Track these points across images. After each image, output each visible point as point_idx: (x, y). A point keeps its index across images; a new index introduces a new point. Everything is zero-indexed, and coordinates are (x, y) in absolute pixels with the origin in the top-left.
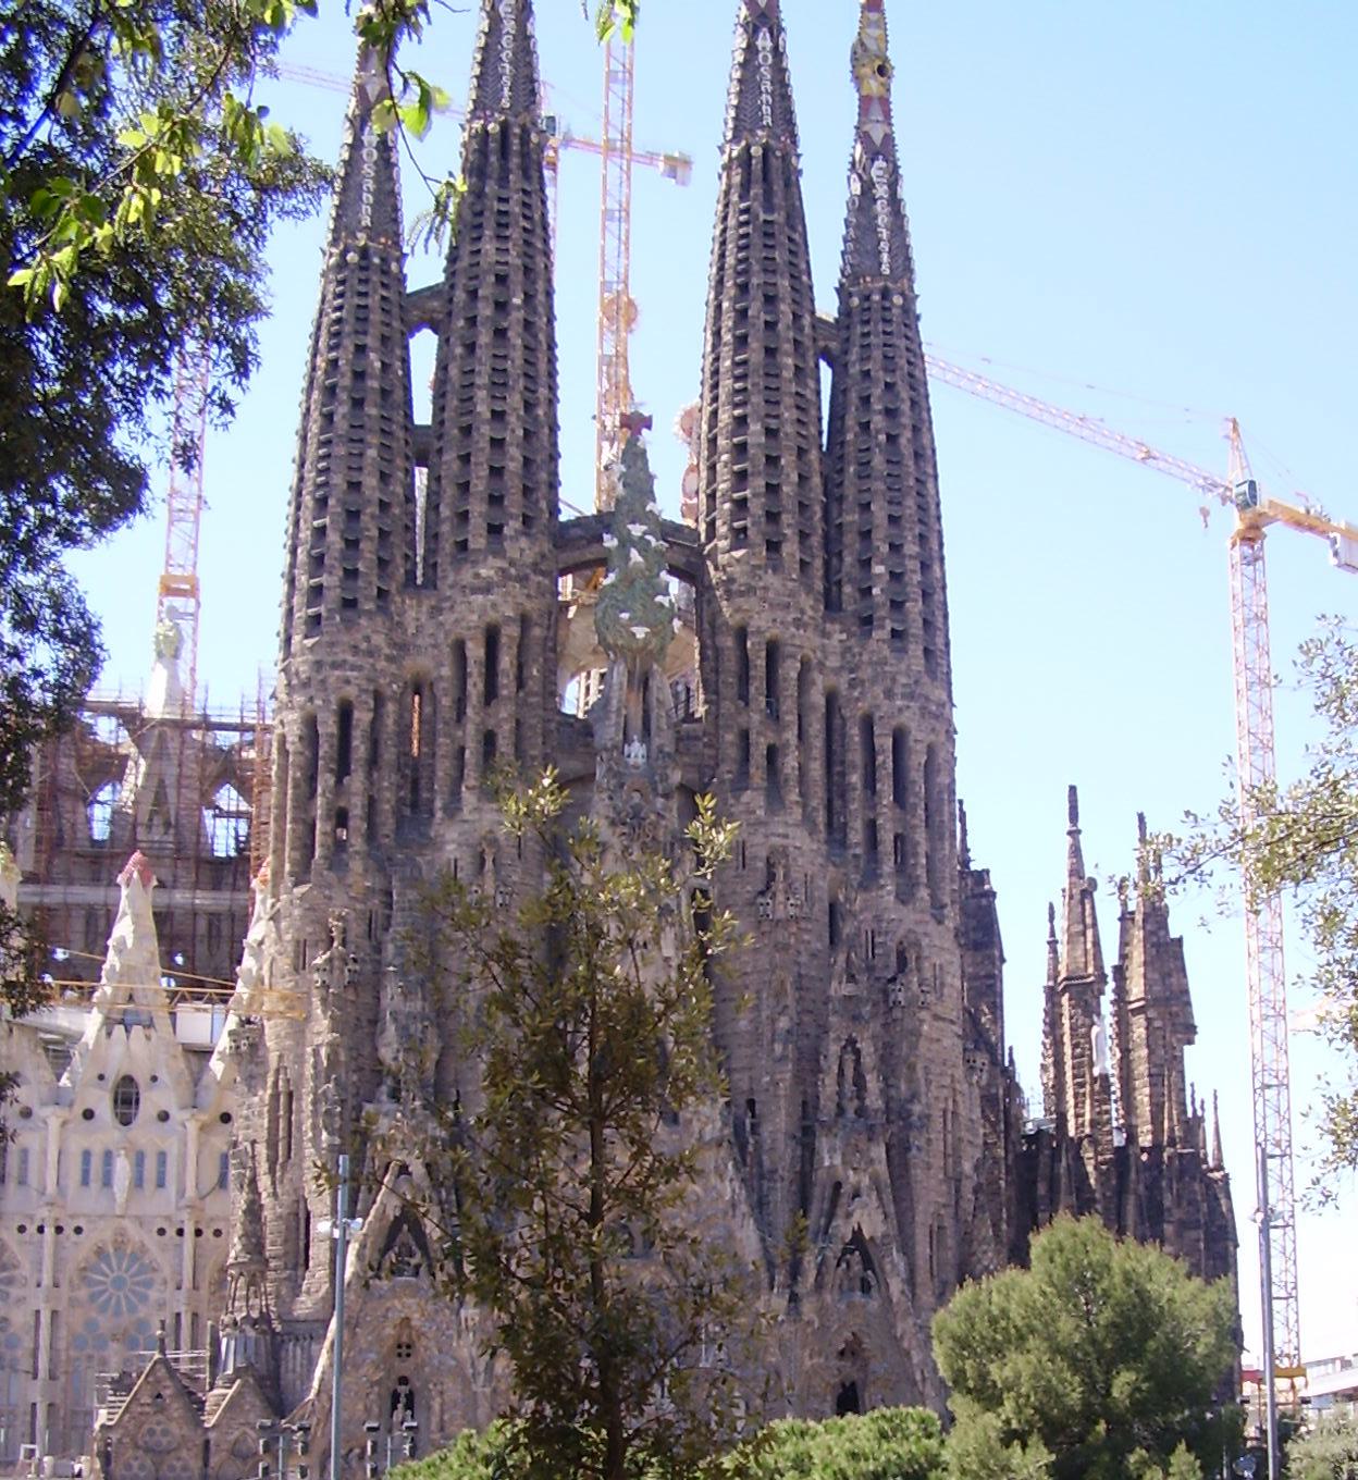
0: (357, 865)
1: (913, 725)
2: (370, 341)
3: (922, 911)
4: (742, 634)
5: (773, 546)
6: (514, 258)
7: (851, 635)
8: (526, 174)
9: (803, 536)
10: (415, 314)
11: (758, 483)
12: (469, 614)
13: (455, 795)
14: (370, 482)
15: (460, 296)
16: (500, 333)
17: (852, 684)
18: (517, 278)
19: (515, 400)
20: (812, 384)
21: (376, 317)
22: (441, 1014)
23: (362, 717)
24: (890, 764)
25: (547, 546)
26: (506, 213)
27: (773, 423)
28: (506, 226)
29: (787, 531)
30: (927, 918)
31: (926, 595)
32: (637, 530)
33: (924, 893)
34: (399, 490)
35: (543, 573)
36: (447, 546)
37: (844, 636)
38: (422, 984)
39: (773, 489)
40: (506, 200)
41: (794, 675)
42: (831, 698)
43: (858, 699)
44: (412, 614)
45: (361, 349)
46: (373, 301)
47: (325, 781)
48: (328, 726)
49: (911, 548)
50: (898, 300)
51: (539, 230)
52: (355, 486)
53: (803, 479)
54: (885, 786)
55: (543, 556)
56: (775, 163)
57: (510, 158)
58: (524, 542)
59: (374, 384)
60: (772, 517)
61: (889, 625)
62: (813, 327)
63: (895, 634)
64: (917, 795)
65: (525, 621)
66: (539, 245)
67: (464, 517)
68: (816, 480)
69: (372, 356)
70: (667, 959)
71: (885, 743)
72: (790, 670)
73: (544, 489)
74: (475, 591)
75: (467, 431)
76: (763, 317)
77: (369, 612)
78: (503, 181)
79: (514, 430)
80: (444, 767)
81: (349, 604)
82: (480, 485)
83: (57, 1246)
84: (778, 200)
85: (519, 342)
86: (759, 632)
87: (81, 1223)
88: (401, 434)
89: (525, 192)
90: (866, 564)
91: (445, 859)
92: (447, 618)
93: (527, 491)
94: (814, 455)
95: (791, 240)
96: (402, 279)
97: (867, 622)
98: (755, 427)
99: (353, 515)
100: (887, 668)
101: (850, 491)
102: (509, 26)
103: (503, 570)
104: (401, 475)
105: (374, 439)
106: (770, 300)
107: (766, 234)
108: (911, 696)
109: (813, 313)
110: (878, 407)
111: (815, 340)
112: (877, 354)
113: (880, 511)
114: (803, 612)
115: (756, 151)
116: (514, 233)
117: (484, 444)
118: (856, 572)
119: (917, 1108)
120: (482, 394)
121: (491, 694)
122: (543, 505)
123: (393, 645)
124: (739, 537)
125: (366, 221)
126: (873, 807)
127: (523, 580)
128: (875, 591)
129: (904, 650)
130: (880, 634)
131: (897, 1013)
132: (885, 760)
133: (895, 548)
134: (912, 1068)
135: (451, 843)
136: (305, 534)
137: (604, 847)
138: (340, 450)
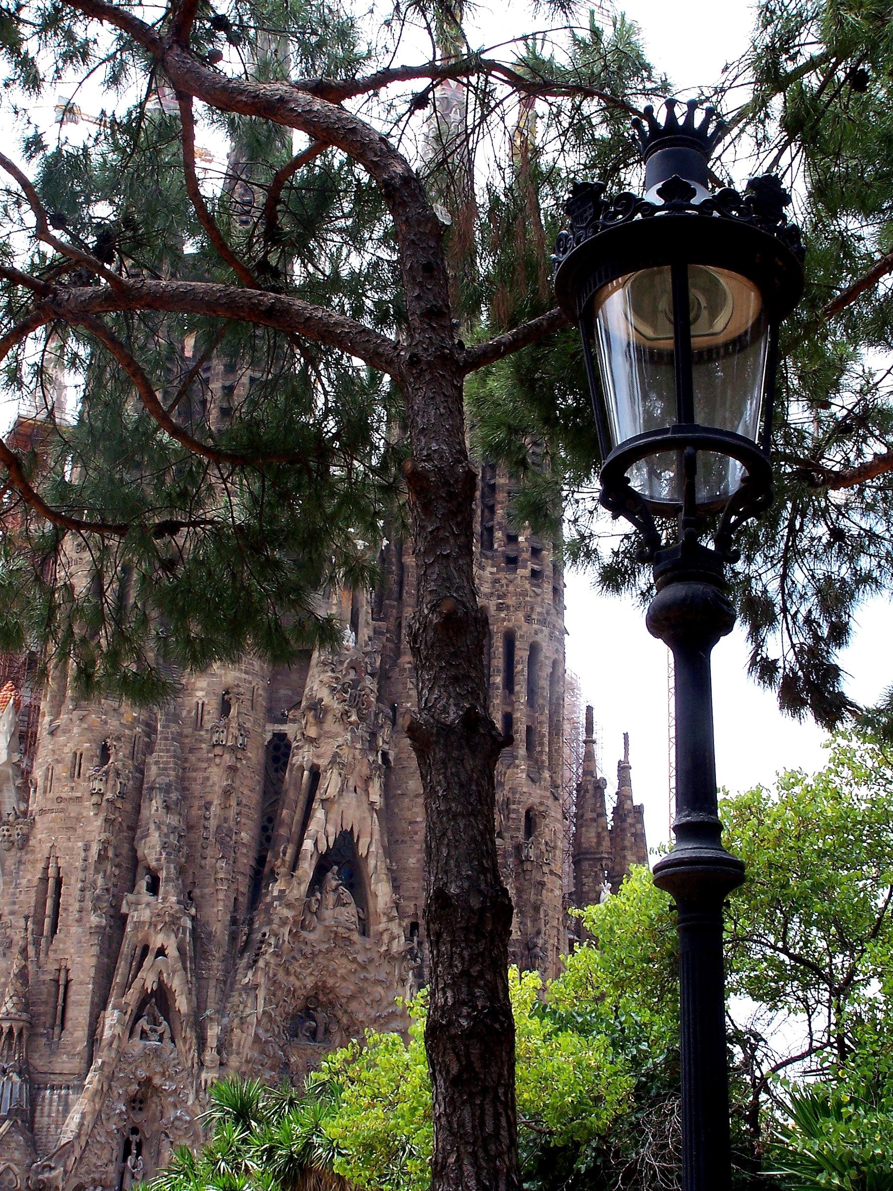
1: (544, 644)
3: (546, 789)
7: (499, 570)
17: (500, 607)
24: (526, 673)
30: (548, 794)
33: (546, 774)
37: (495, 570)
43: (504, 620)
54: (521, 688)
63: (535, 574)
64: (544, 698)
70: (372, 803)
71: (522, 654)
91: (196, 700)
97: (512, 562)
100: (528, 599)
119: (540, 942)
126: (512, 704)
128: (521, 539)
131: (527, 866)
132: (521, 668)
134: (537, 909)
137: (326, 710)
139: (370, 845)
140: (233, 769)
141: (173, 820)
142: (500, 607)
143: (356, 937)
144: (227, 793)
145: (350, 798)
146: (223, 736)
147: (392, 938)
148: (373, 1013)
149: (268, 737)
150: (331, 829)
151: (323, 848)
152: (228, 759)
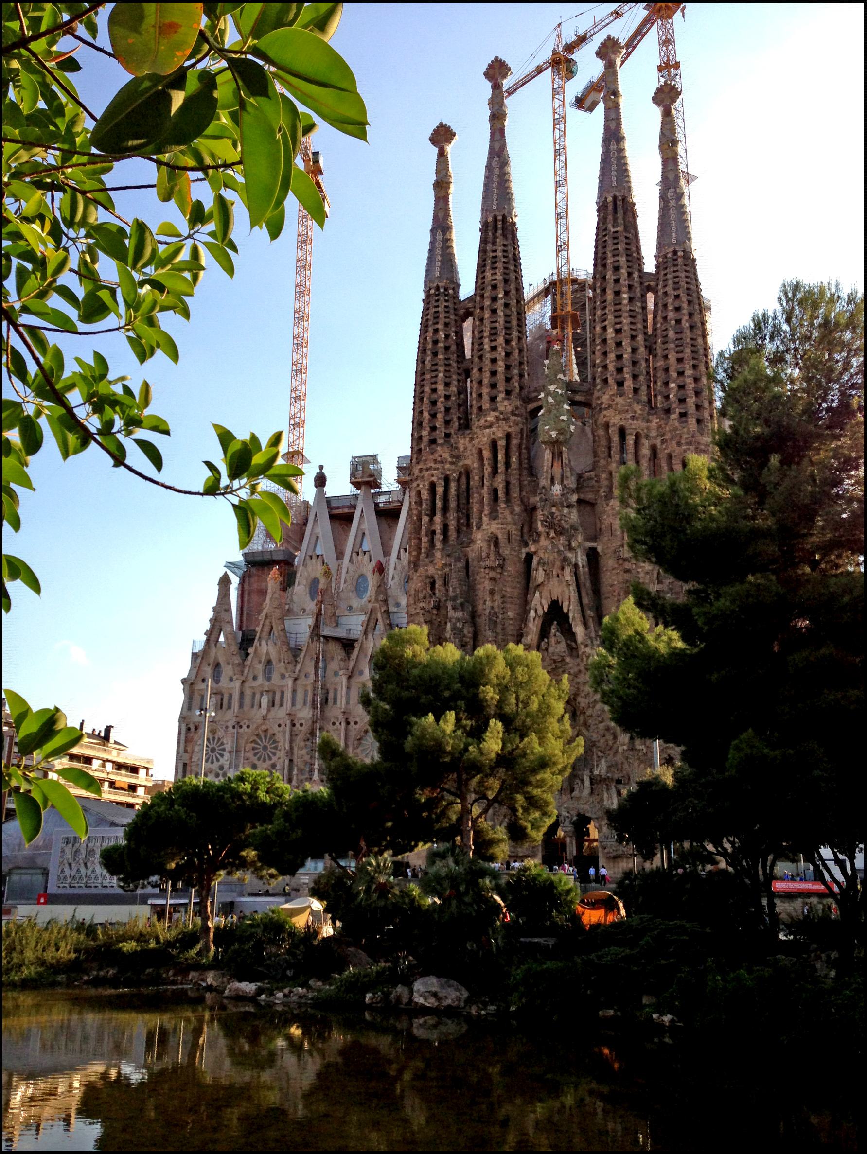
0: (438, 554)
2: (440, 326)
4: (607, 426)
6: (499, 277)
8: (504, 235)
9: (635, 377)
10: (462, 312)
11: (612, 356)
12: (483, 438)
13: (481, 518)
14: (441, 387)
15: (478, 298)
16: (494, 311)
17: (663, 442)
18: (501, 285)
19: (501, 340)
20: (639, 304)
21: (442, 316)
22: (474, 615)
23: (440, 490)
25: (518, 403)
26: (496, 257)
27: (618, 326)
28: (496, 262)
29: (627, 376)
31: (697, 393)
32: (552, 388)
34: (455, 389)
35: (515, 415)
36: (475, 410)
38: (462, 604)
39: (619, 357)
40: (495, 251)
41: (632, 442)
42: (654, 450)
44: (462, 442)
45: (436, 331)
46: (441, 309)
47: (425, 519)
49: (689, 372)
50: (680, 254)
51: (512, 262)
52: (434, 391)
53: (634, 350)
55: (517, 408)
56: (619, 203)
57: (499, 231)
58: (506, 403)
59: (441, 345)
60: (620, 370)
61: (678, 411)
62: (640, 277)
63: (683, 415)
65: (508, 436)
66: (512, 268)
67: (480, 395)
68: (642, 349)
69: (441, 333)
72: (630, 440)
73: (517, 378)
74: (486, 427)
75: (481, 357)
76: (614, 277)
77: (442, 445)
78: (494, 243)
79: (501, 353)
80: (475, 508)
81: (433, 442)
82: (486, 381)
83: (346, 730)
84: (620, 221)
85: (501, 314)
86: (614, 425)
87: (358, 720)
88: (455, 364)
89: (504, 245)
90: (666, 384)
92: (475, 442)
93: (508, 380)
94: (640, 338)
95: (627, 238)
96: (456, 295)
97: (668, 411)
98: (610, 330)
99: (434, 403)
101: (659, 351)
102: (497, 171)
103: (497, 417)
104: (455, 383)
105: (442, 369)
106: (617, 269)
107: (615, 238)
108: (690, 443)
109: (640, 270)
110: (671, 308)
111: (641, 283)
112: (670, 282)
113: (672, 357)
114: (635, 412)
115: (610, 199)
116: (500, 265)
117: (488, 362)
118: (663, 389)
120: (486, 340)
121: (495, 472)
122: (516, 384)
123: (452, 456)
125: (438, 274)
127: (506, 419)
129: (686, 422)
130: (674, 416)
133: (681, 374)
135: (479, 540)
137: (539, 535)
139: (571, 607)
140: (493, 579)
141: (459, 614)
143: (568, 659)
144: (492, 592)
145: (554, 581)
146: (487, 563)
147: (588, 657)
148: (587, 701)
149: (524, 556)
150: (544, 602)
151: (540, 612)
152: (492, 574)
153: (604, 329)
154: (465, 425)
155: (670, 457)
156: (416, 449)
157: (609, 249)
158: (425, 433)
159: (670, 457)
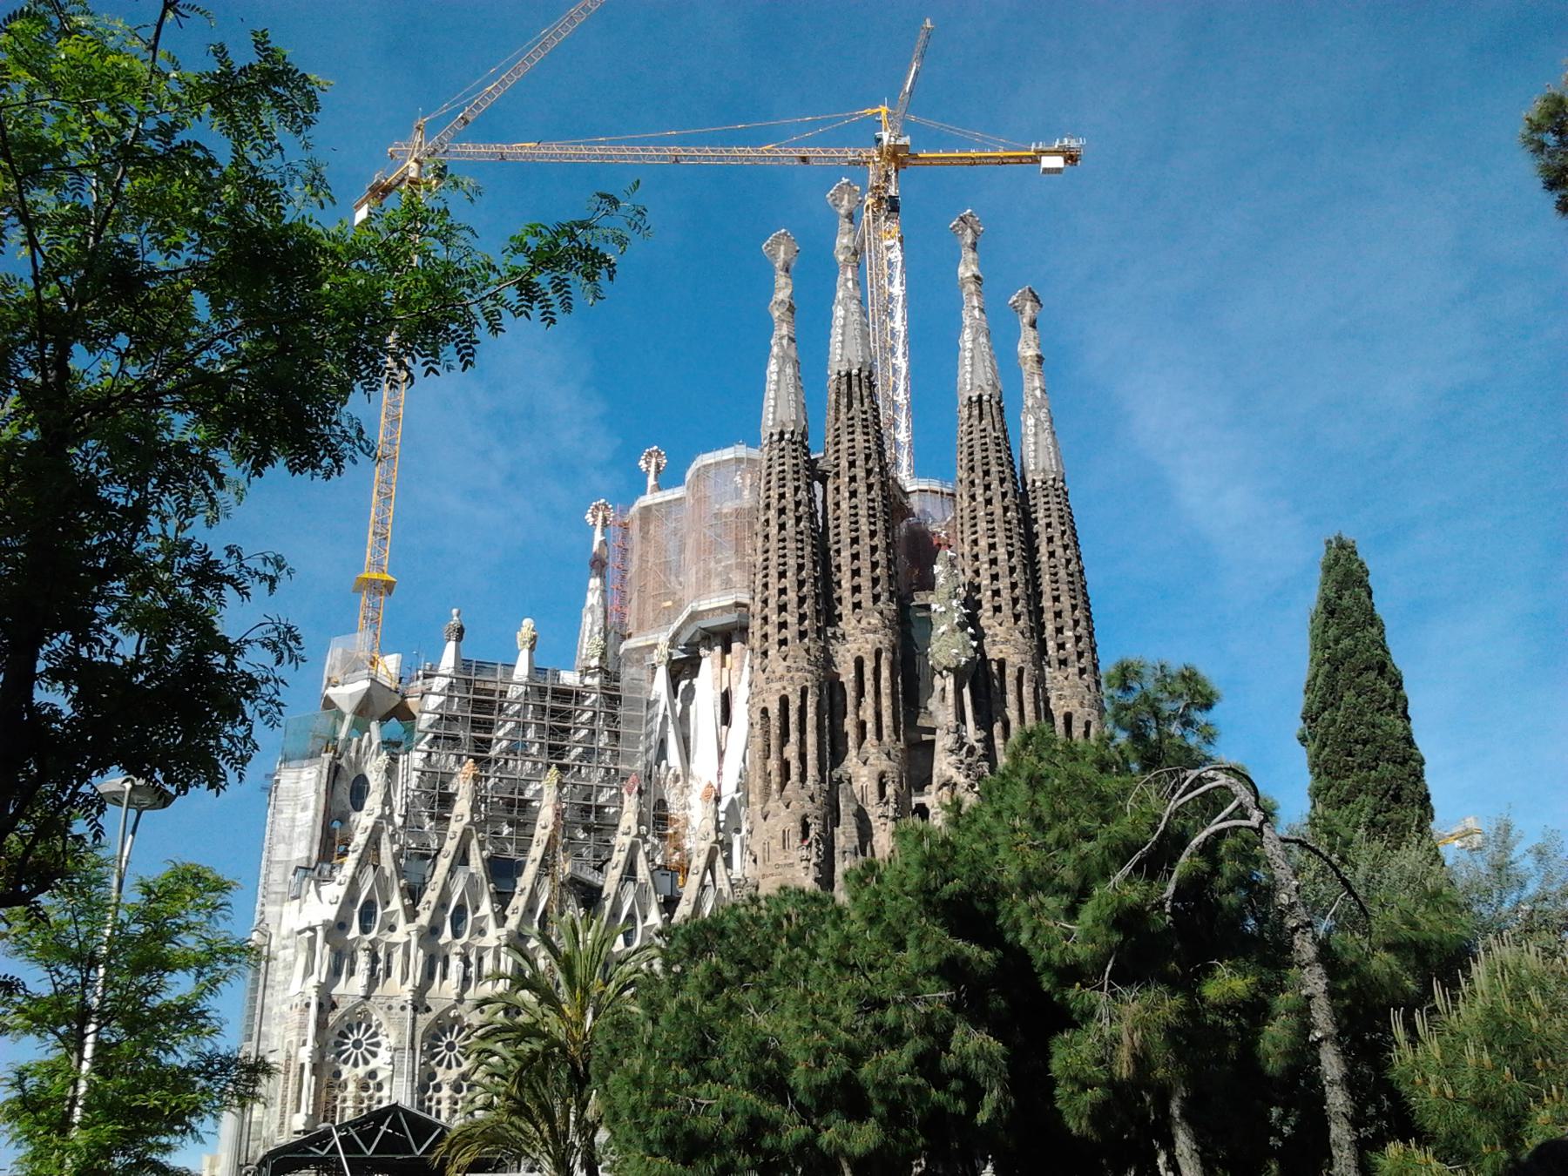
5: (1017, 617)
17: (1060, 697)
19: (880, 524)
23: (811, 701)
48: (794, 704)
74: (868, 631)
120: (863, 521)
124: (997, 609)
130: (1072, 670)
136: (773, 591)
138: (791, 545)
142: (1060, 697)
153: (992, 546)
154: (832, 619)
155: (1068, 718)
156: (777, 638)
157: (992, 455)
158: (792, 619)
159: (1068, 718)
